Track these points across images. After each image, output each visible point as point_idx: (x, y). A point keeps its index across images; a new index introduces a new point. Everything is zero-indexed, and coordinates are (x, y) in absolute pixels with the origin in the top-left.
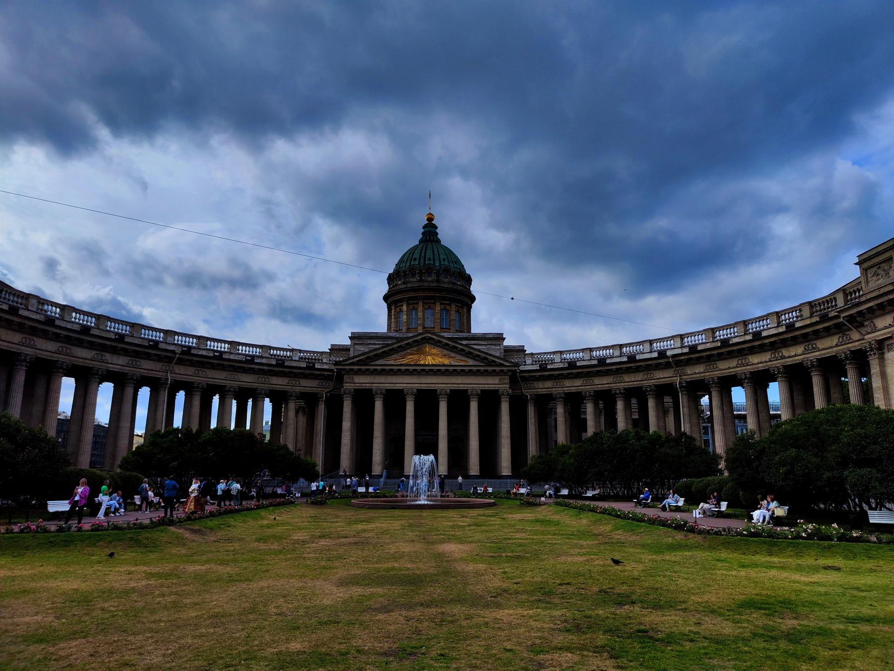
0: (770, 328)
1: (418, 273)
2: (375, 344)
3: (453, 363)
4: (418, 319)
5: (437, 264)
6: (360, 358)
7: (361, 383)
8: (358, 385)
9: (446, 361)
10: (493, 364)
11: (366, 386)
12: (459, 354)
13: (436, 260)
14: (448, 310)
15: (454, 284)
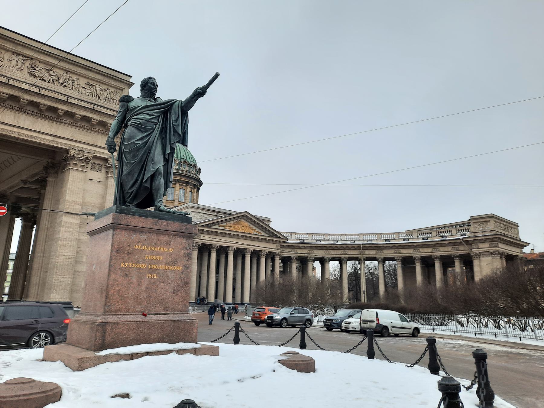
0: (413, 238)
1: (177, 164)
2: (204, 213)
3: (255, 233)
4: (174, 195)
5: (189, 160)
6: (208, 223)
7: (205, 240)
8: (203, 241)
9: (252, 232)
10: (274, 236)
11: (207, 242)
12: (258, 228)
13: (187, 157)
14: (192, 192)
15: (197, 176)
